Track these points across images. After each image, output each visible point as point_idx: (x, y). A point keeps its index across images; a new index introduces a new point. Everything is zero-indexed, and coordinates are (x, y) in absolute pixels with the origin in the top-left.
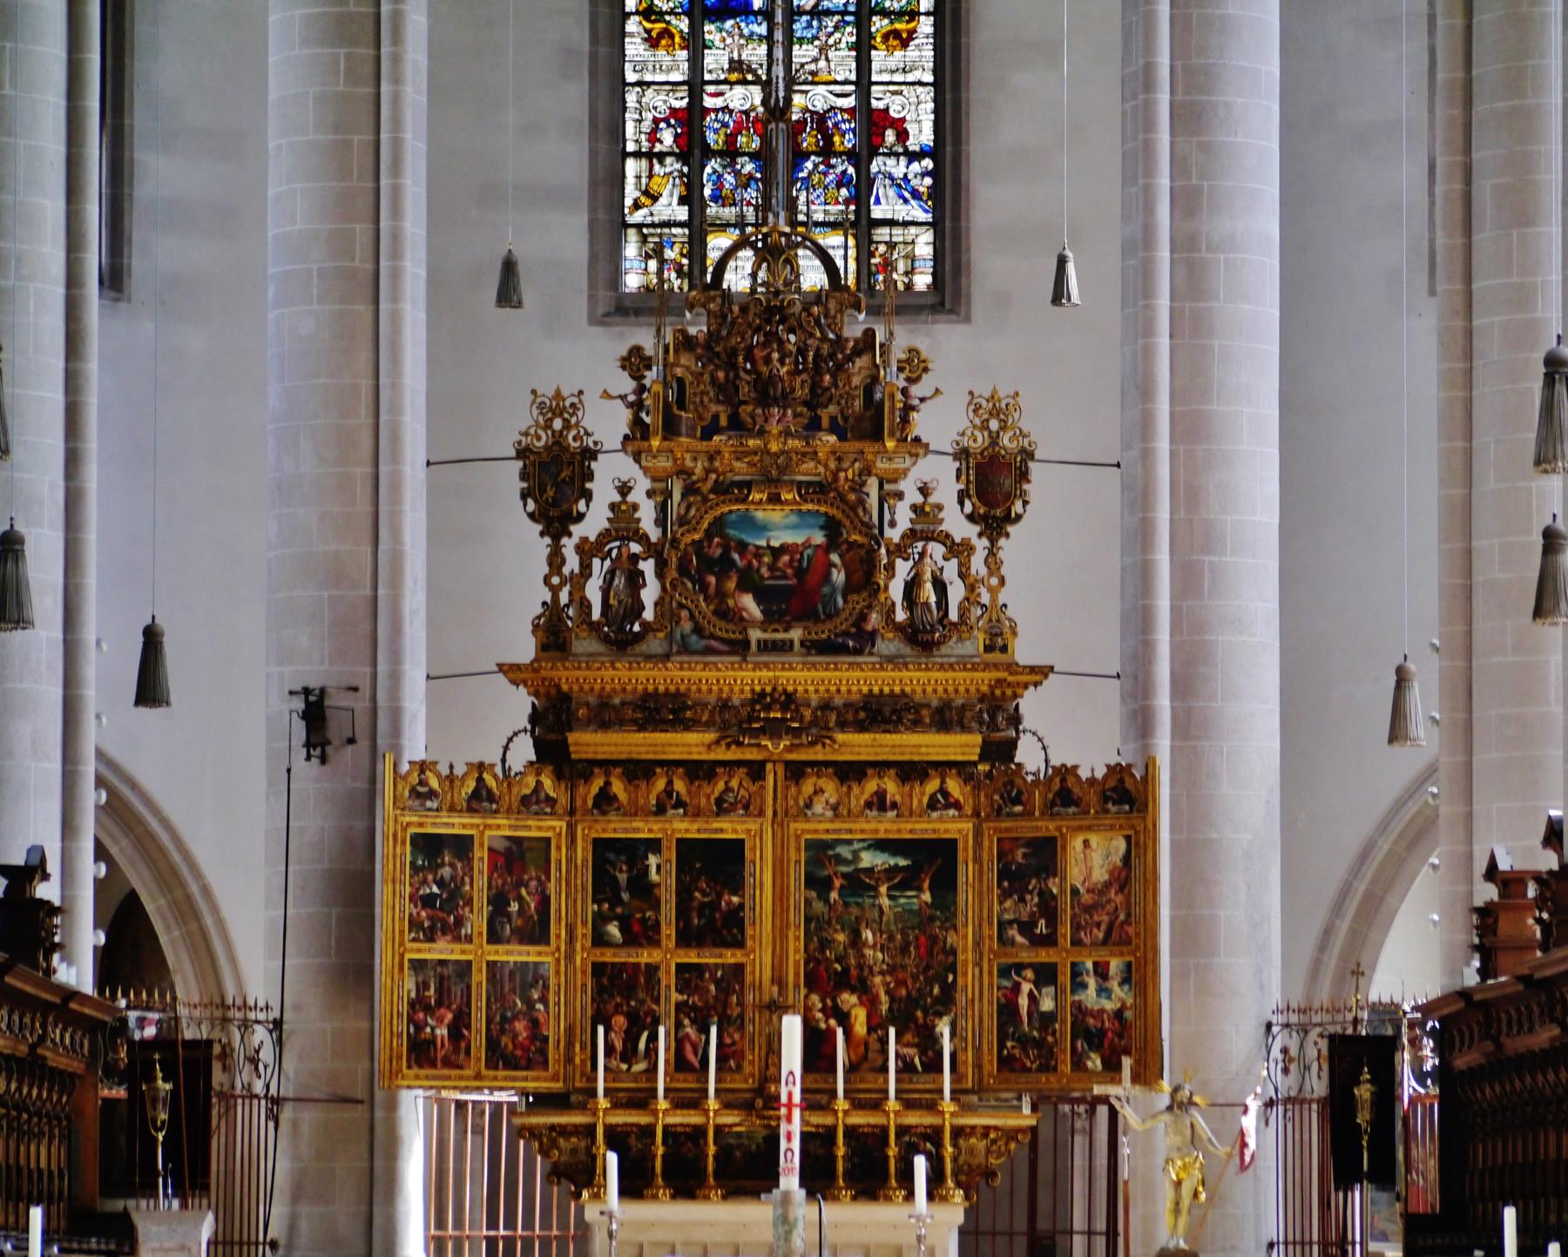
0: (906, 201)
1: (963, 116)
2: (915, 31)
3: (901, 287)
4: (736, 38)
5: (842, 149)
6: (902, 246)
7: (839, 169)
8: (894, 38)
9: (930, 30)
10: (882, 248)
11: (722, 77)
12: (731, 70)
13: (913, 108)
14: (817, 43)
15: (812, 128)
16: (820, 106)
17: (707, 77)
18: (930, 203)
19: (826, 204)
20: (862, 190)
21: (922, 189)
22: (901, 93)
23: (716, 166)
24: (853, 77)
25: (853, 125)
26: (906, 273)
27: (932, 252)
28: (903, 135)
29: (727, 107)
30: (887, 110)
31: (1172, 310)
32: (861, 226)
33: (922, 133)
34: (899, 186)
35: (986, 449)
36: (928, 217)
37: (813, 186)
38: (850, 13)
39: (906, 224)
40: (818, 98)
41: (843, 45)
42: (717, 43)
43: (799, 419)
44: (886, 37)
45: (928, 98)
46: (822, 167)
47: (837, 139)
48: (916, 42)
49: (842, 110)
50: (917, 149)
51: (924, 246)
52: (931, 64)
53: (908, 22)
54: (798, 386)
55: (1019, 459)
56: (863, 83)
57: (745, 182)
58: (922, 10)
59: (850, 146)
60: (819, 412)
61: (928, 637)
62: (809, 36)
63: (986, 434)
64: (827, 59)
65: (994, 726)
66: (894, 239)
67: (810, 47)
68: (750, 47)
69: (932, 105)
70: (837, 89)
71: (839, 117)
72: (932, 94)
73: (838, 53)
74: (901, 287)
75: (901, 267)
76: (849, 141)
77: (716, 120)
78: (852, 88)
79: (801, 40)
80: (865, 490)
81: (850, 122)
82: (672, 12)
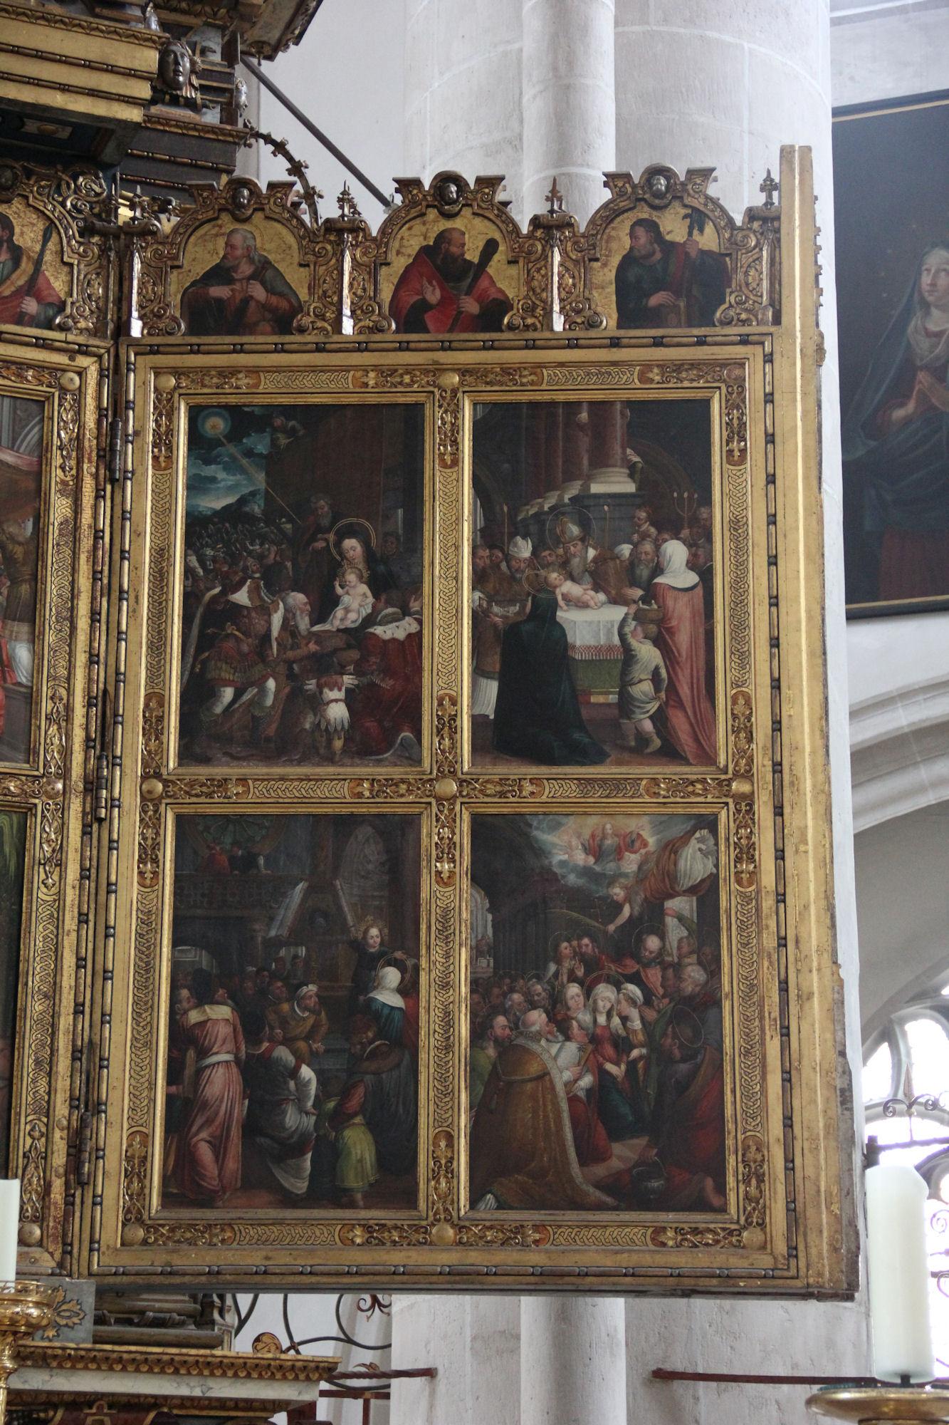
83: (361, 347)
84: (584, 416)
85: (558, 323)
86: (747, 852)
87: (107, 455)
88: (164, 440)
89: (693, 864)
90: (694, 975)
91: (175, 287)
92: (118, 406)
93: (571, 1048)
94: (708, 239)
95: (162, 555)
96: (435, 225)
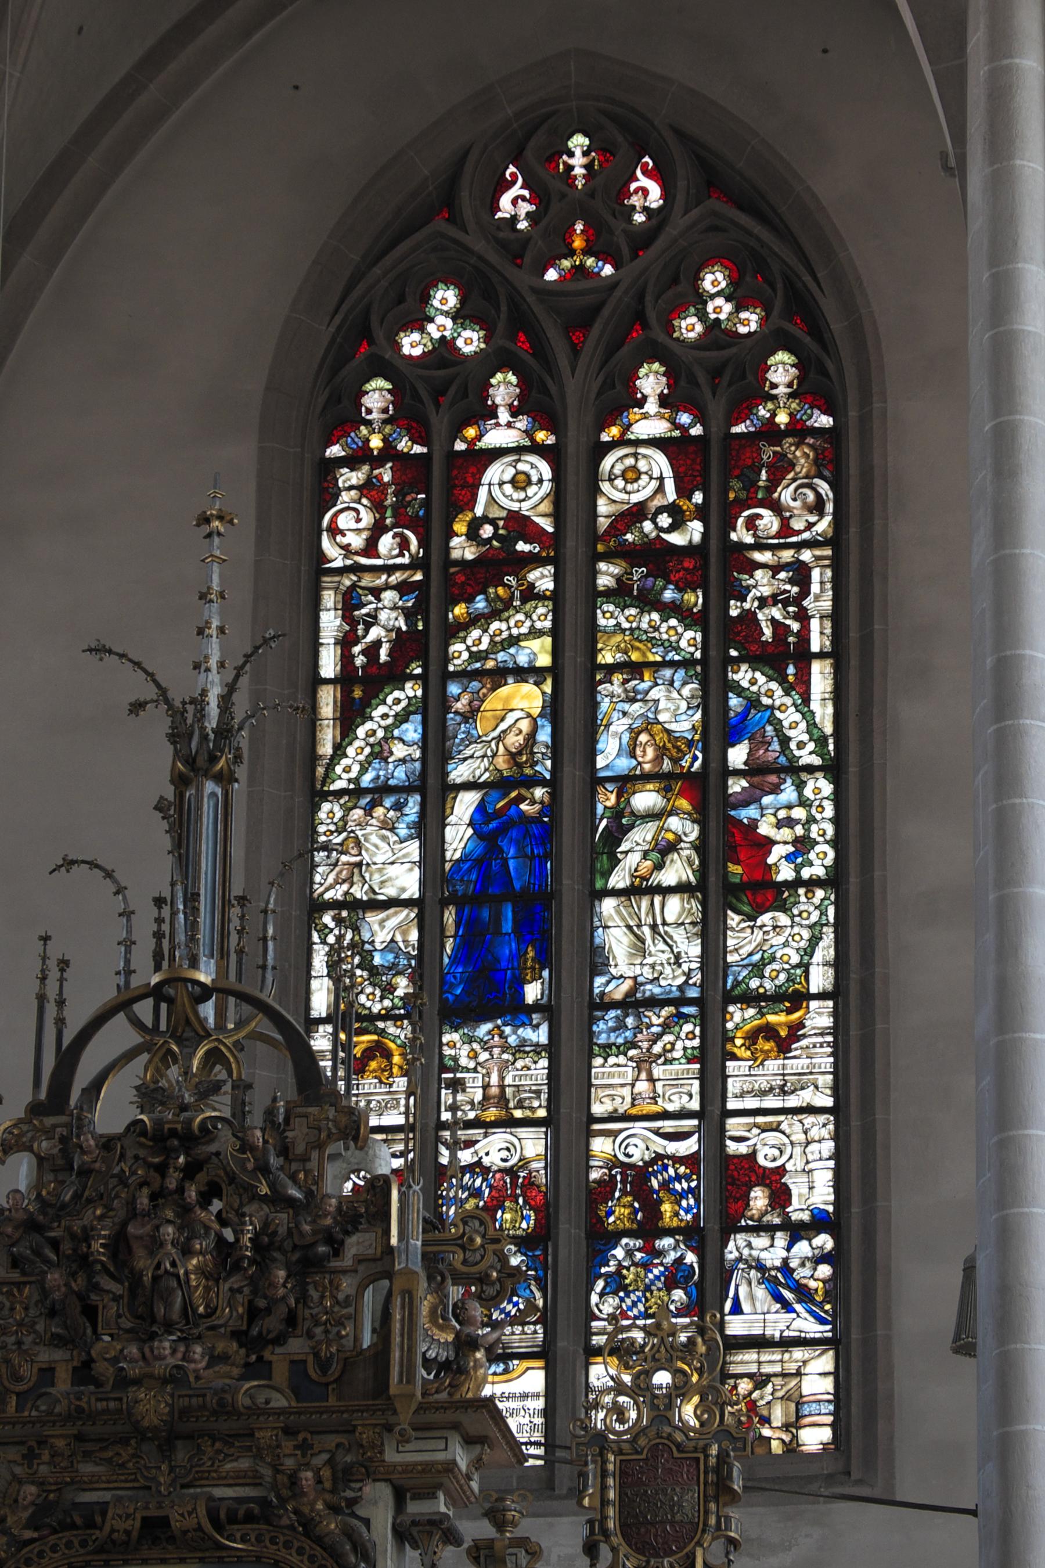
0: (787, 1307)
1: (879, 1151)
2: (801, 1025)
4: (496, 1051)
5: (675, 1223)
6: (778, 1381)
7: (672, 1256)
8: (767, 1039)
9: (827, 1021)
10: (744, 1386)
11: (471, 1115)
13: (798, 1150)
14: (632, 1053)
16: (638, 1154)
21: (813, 1284)
22: (777, 1128)
24: (695, 1105)
25: (693, 1184)
26: (786, 1427)
27: (830, 1388)
28: (781, 1197)
29: (479, 1163)
30: (753, 1154)
38: (691, 1002)
39: (787, 1343)
41: (678, 1054)
42: (464, 1061)
43: (223, 1368)
44: (752, 1037)
45: (825, 1133)
46: (639, 1255)
47: (666, 1208)
48: (804, 1043)
50: (806, 1216)
53: (789, 1011)
54: (222, 1302)
58: (813, 990)
59: (689, 1217)
60: (267, 1355)
64: (651, 1080)
66: (767, 1369)
67: (622, 1060)
68: (519, 1064)
69: (831, 1144)
71: (671, 1171)
72: (831, 1127)
74: (776, 1447)
75: (778, 1416)
78: (695, 1122)
79: (607, 1050)
80: (361, 1512)
81: (688, 1179)
82: (384, 1018)
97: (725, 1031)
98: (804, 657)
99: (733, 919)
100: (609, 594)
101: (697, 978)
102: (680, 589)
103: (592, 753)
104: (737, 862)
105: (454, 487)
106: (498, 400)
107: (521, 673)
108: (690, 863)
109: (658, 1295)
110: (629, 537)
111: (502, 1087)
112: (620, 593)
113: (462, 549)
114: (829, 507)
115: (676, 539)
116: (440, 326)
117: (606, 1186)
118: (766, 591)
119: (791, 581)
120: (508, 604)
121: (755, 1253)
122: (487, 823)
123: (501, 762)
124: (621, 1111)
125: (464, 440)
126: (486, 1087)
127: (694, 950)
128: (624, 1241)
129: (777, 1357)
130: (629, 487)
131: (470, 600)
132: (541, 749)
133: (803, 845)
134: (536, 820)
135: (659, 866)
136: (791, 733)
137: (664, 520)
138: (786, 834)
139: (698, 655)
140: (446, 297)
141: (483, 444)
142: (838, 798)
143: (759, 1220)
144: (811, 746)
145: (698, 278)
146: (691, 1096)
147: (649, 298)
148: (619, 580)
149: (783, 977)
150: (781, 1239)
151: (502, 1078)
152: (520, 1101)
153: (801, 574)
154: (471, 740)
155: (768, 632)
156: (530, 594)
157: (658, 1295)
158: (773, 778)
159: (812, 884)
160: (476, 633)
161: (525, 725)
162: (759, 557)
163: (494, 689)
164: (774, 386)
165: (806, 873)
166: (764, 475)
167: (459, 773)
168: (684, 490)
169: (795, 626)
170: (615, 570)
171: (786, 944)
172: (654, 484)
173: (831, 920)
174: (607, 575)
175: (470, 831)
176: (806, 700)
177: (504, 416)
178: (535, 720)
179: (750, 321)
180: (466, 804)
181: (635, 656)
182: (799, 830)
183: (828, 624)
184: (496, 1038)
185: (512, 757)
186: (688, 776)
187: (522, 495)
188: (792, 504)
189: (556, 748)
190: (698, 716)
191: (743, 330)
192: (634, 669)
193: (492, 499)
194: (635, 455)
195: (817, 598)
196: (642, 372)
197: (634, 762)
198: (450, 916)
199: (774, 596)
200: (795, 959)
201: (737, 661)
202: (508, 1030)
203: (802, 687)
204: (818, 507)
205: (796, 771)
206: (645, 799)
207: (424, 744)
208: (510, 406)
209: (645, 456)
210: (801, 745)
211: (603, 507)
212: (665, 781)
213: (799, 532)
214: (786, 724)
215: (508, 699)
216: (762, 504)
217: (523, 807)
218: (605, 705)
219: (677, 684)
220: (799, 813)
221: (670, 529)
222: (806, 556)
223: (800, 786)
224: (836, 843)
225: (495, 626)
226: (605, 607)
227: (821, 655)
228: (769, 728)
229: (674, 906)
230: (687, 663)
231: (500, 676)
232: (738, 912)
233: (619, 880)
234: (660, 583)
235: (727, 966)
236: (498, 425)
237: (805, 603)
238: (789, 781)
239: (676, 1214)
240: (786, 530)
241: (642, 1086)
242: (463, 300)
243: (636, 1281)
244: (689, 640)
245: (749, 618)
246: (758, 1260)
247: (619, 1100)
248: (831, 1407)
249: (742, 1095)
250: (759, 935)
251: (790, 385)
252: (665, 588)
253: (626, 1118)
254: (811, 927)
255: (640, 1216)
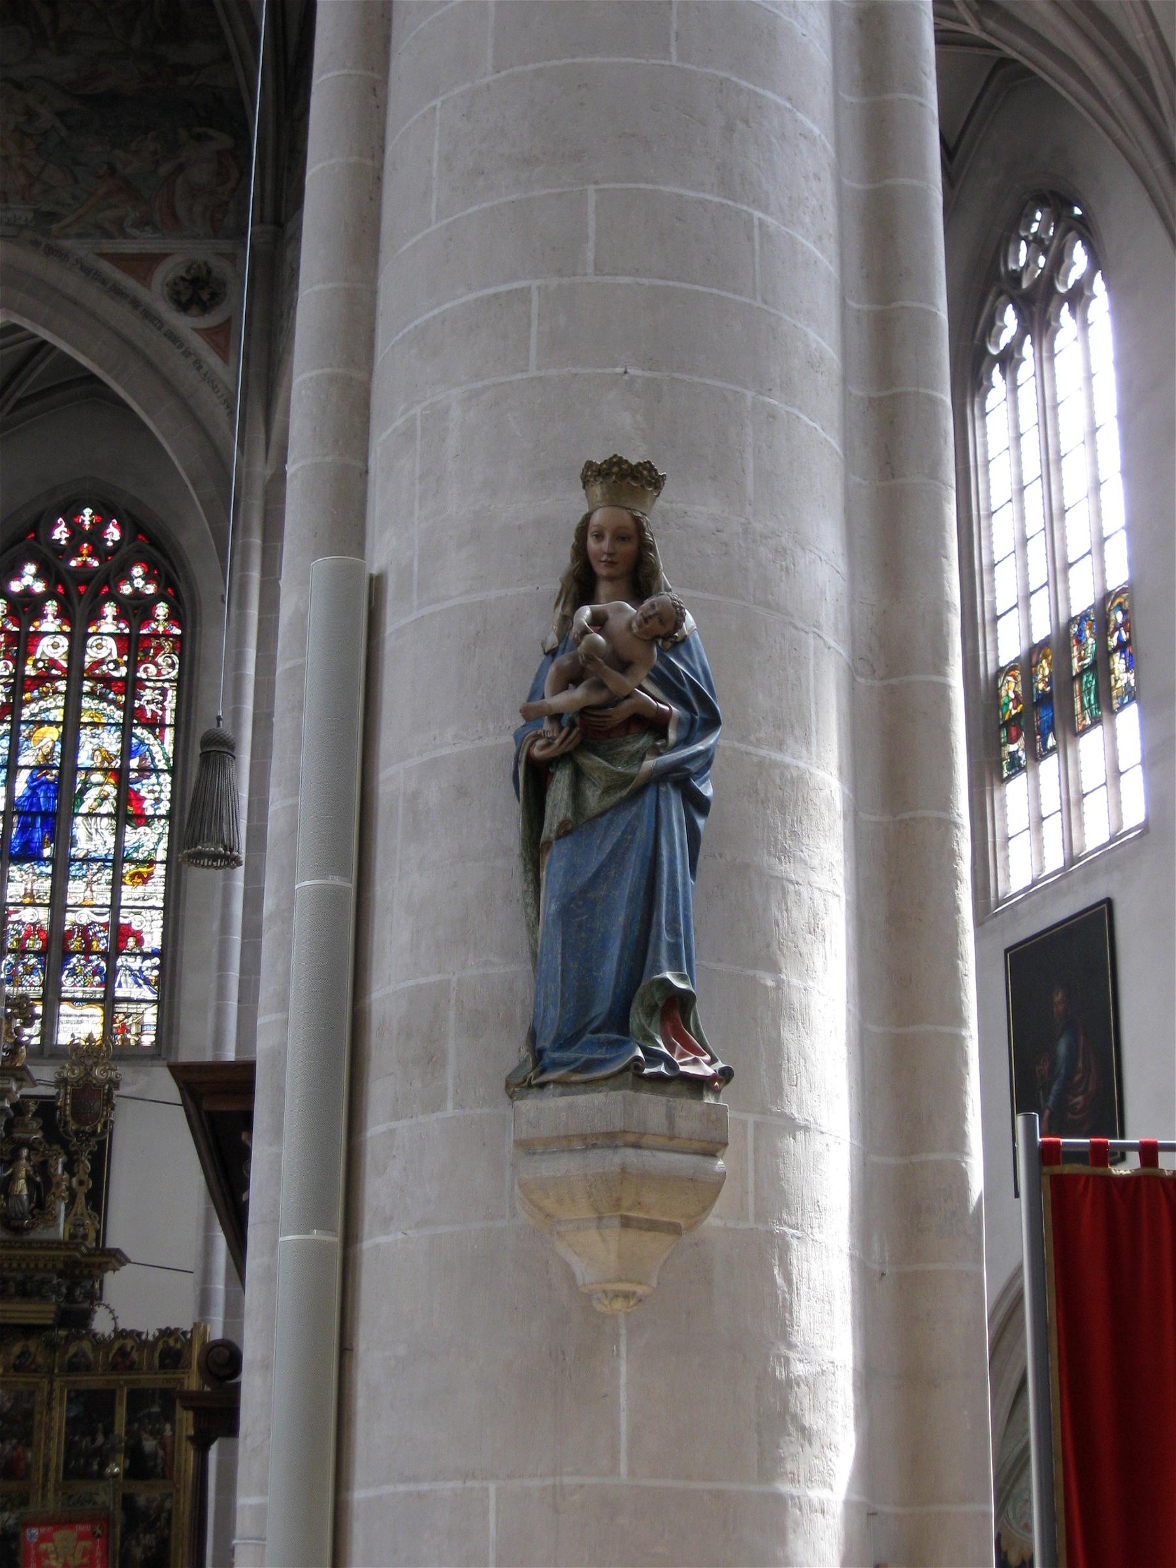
0: (140, 986)
2: (152, 873)
3: (132, 1043)
4: (31, 875)
5: (98, 950)
6: (135, 1016)
8: (139, 878)
9: (164, 873)
10: (121, 1017)
11: (19, 900)
12: (25, 896)
13: (148, 923)
14: (85, 879)
15: (78, 936)
16: (84, 921)
17: (9, 900)
18: (156, 987)
19: (84, 986)
20: (109, 979)
21: (151, 978)
22: (139, 914)
23: (11, 959)
24: (108, 902)
25: (106, 934)
26: (137, 1034)
27: (155, 1020)
28: (140, 942)
30: (130, 925)
31: (241, 981)
32: (109, 1002)
33: (153, 940)
34: (135, 975)
35: (81, 1078)
36: (153, 997)
37: (76, 974)
40: (84, 917)
41: (103, 881)
42: (18, 878)
44: (133, 877)
46: (82, 962)
47: (94, 943)
48: (153, 880)
49: (100, 924)
50: (149, 950)
51: (150, 1016)
52: (162, 895)
53: (148, 867)
55: (107, 1087)
56: (115, 907)
57: (30, 971)
58: (158, 859)
59: (103, 948)
61: (16, 1223)
62: (80, 874)
63: (82, 1068)
64: (92, 891)
65: (70, 1297)
66: (130, 1011)
68: (40, 881)
69: (162, 922)
70: (97, 910)
72: (162, 915)
73: (99, 886)
74: (132, 1043)
75: (134, 1030)
76: (103, 945)
77: (13, 929)
78: (108, 909)
83: (103, 1375)
84: (150, 1392)
85: (145, 1368)
86: (178, 1502)
87: (49, 1404)
88: (61, 1398)
89: (167, 1505)
90: (166, 1532)
91: (68, 1356)
92: (51, 1392)
93: (140, 1549)
94: (179, 1346)
95: (60, 1429)
96: (121, 1341)
97: (122, 874)
98: (163, 726)
99: (128, 828)
100: (88, 694)
101: (112, 851)
102: (115, 694)
103: (76, 757)
104: (131, 806)
105: (28, 646)
106: (49, 612)
107: (51, 723)
108: (113, 805)
109: (89, 978)
110: (97, 671)
111: (32, 890)
112: (92, 694)
113: (30, 671)
114: (177, 666)
115: (116, 674)
116: (27, 580)
117: (71, 932)
118: (150, 698)
119: (160, 695)
120: (47, 694)
121: (129, 964)
122: (33, 782)
123: (40, 758)
124: (79, 903)
125: (34, 627)
126: (26, 889)
127: (113, 839)
128: (77, 955)
129: (135, 1006)
130: (99, 651)
131: (32, 692)
132: (56, 754)
133: (158, 801)
134: (52, 783)
135: (100, 805)
136: (155, 755)
137: (112, 666)
138: (151, 796)
139: (121, 721)
140: (30, 569)
141: (40, 629)
142: (173, 783)
143: (131, 950)
144: (164, 761)
145: (130, 569)
146: (107, 898)
147: (111, 577)
148: (91, 688)
149: (146, 853)
150: (139, 959)
151: (32, 886)
152: (40, 896)
153: (164, 692)
154: (28, 748)
155: (149, 715)
156: (56, 692)
157: (89, 978)
158: (148, 774)
159: (160, 817)
160: (33, 705)
161: (50, 744)
162: (148, 684)
163: (39, 728)
164: (158, 616)
165: (158, 812)
166: (152, 651)
167: (22, 761)
168: (120, 655)
169: (160, 713)
170: (91, 684)
171: (148, 840)
172: (109, 651)
173: (167, 832)
174: (87, 686)
175: (26, 785)
176: (163, 743)
177: (50, 618)
178: (54, 742)
179: (151, 589)
180: (24, 776)
181: (96, 720)
182: (157, 795)
183: (173, 713)
184: (31, 870)
185: (45, 756)
186: (113, 770)
187: (55, 651)
188: (163, 664)
189: (63, 755)
190: (120, 745)
191: (148, 592)
192: (95, 725)
193: (43, 653)
194: (102, 639)
195: (170, 702)
196: (107, 605)
197: (93, 762)
198: (15, 819)
199: (153, 700)
200: (152, 847)
201: (136, 725)
202: (36, 867)
203: (160, 737)
204: (172, 666)
205: (157, 771)
206: (97, 777)
207: (10, 748)
208: (53, 615)
209: (106, 640)
210: (159, 761)
211: (87, 659)
212: (105, 771)
213: (164, 675)
214: (154, 752)
215: (44, 733)
216: (150, 663)
217: (48, 777)
218: (83, 738)
219: (112, 732)
220: (157, 788)
221: (113, 670)
222: (167, 685)
223: (158, 777)
224: (170, 801)
225: (42, 703)
226: (86, 699)
227: (170, 726)
228: (147, 753)
229: (105, 821)
230: (116, 724)
231: (41, 723)
232: (130, 826)
233: (84, 809)
234: (108, 691)
235: (125, 847)
236: (47, 622)
237: (165, 704)
238: (154, 775)
239: (98, 946)
240: (159, 673)
241: (88, 893)
242: (38, 570)
243: (80, 972)
244: (118, 715)
245: (142, 708)
246: (130, 967)
247: (78, 899)
248: (155, 1028)
249: (128, 899)
250: (137, 836)
251: (165, 616)
252: (109, 693)
253: (81, 906)
254: (159, 834)
255: (84, 946)
